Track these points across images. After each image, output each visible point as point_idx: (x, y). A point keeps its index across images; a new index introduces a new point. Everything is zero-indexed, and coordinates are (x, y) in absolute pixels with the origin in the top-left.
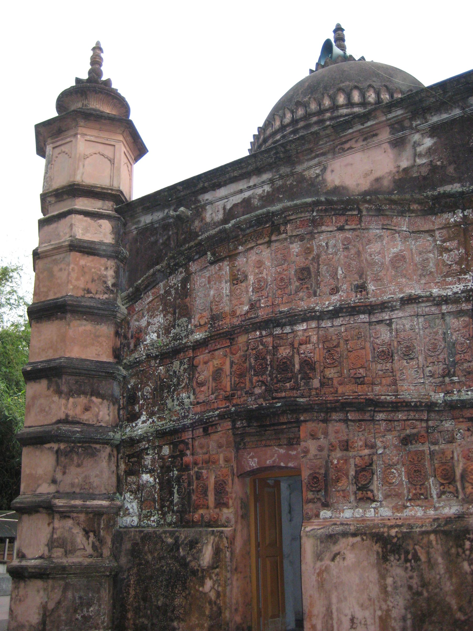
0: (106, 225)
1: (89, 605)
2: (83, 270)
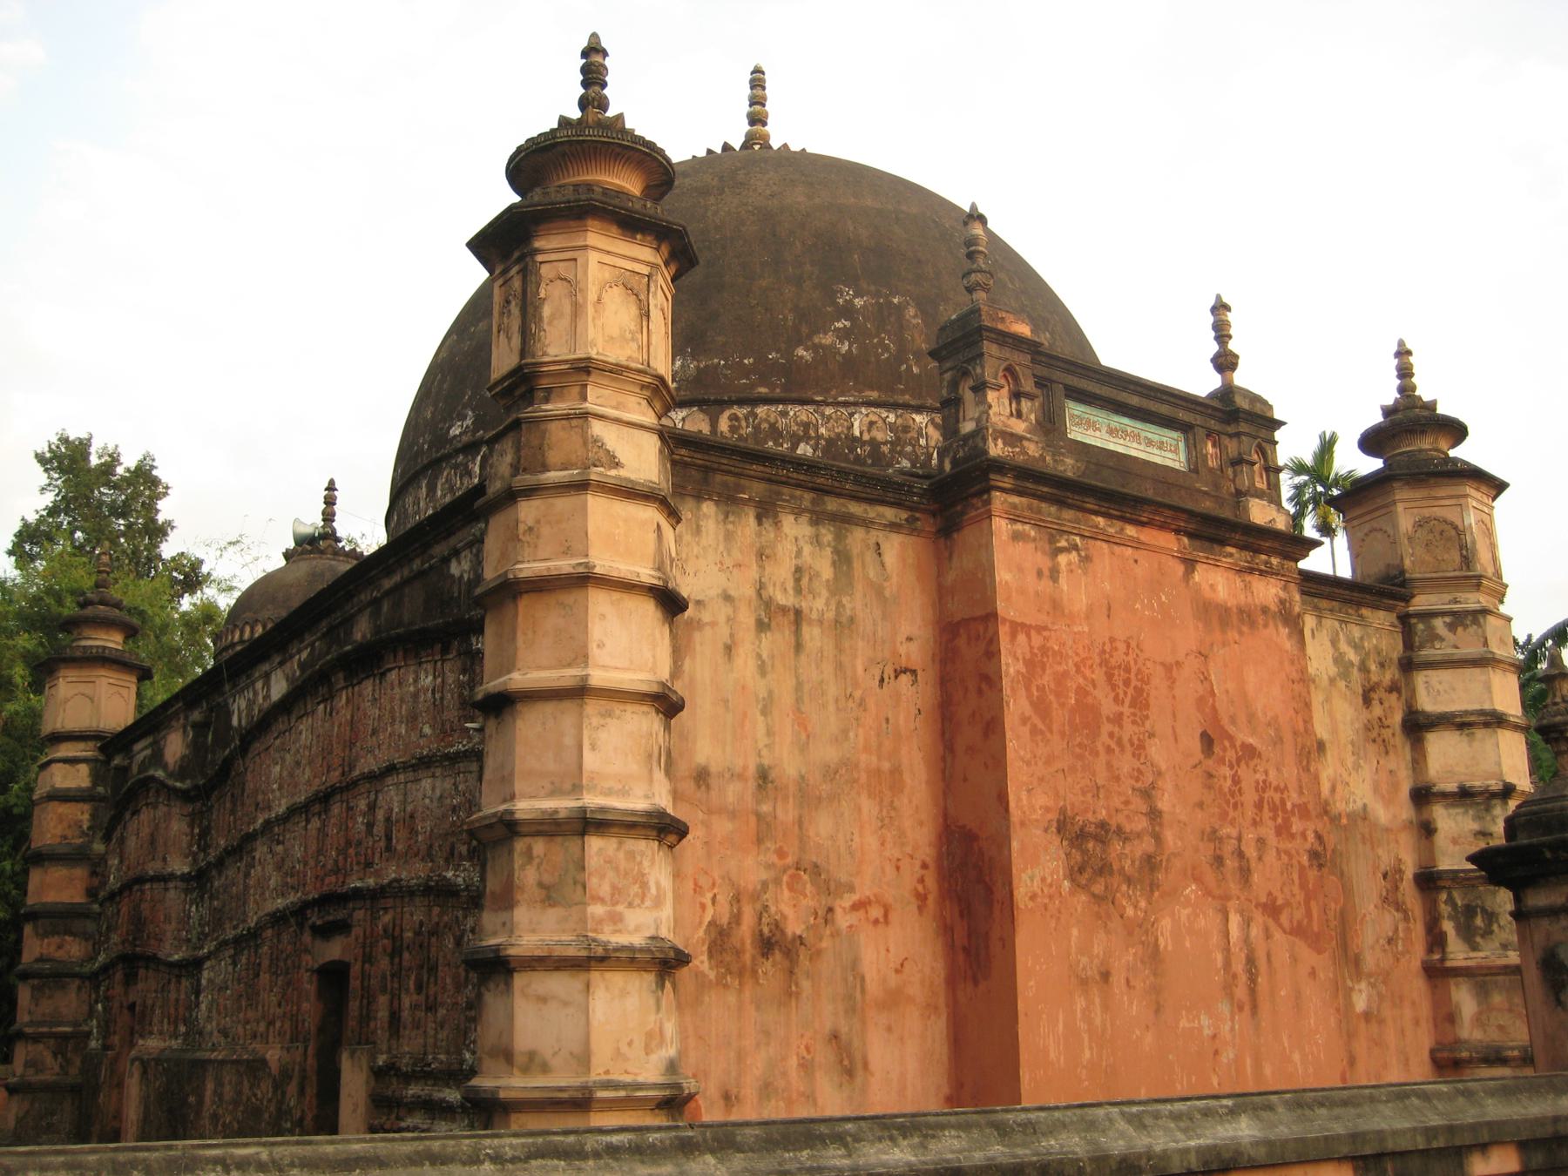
0: (84, 769)
1: (52, 1114)
2: (61, 819)
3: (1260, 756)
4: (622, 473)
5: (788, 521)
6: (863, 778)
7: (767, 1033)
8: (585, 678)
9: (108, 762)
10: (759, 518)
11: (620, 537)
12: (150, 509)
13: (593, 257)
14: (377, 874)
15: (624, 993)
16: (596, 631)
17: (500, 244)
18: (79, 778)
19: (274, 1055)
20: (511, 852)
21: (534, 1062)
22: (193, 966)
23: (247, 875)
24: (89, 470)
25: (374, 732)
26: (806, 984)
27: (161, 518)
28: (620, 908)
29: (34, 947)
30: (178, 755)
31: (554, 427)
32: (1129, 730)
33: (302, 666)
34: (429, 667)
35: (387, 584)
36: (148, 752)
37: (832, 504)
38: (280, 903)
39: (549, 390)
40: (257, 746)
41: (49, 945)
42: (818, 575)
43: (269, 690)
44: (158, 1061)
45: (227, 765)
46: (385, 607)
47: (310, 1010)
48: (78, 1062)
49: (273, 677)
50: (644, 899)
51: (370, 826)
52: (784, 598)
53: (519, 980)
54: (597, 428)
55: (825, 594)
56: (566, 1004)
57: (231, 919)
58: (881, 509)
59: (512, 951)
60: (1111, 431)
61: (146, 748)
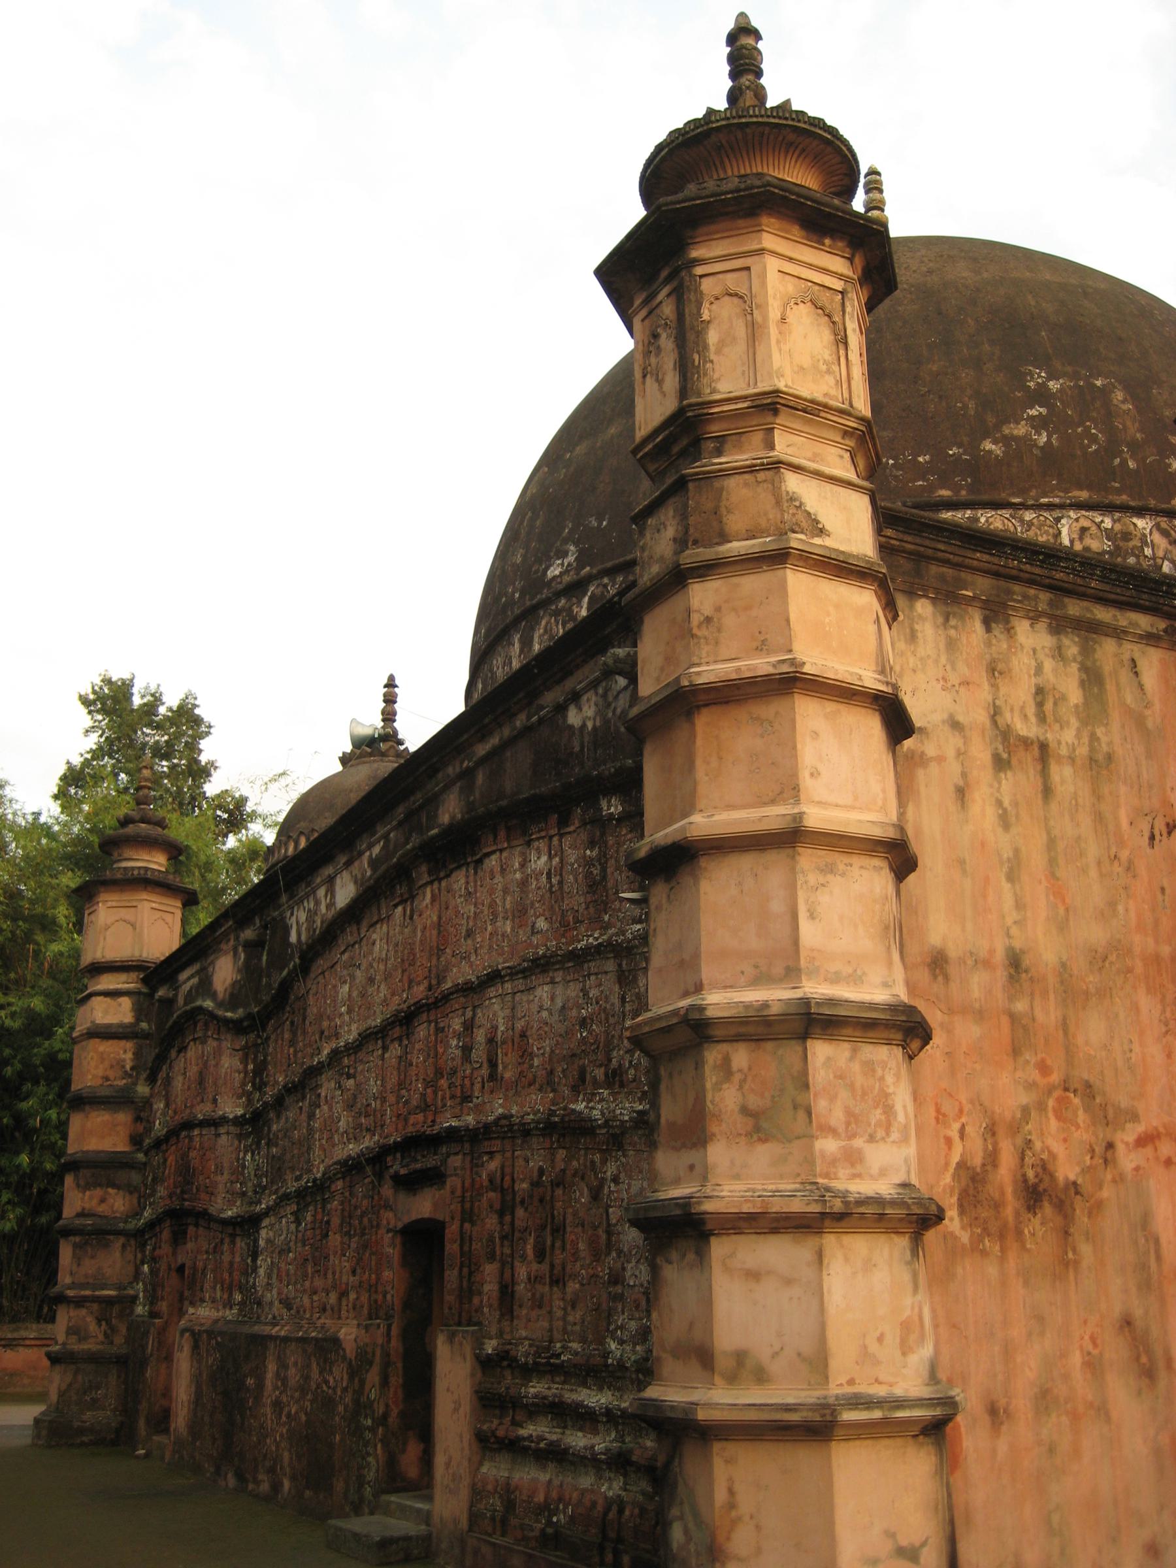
0: (126, 1003)
1: (98, 1388)
4: (828, 542)
5: (1022, 627)
6: (1139, 968)
7: (1040, 1319)
8: (801, 815)
9: (151, 995)
10: (987, 623)
11: (832, 626)
12: (193, 748)
13: (772, 265)
14: (478, 1109)
15: (869, 1266)
16: (808, 754)
17: (641, 272)
18: (120, 1012)
19: (349, 1333)
20: (699, 1065)
21: (745, 1367)
22: (249, 1224)
23: (311, 1116)
24: (133, 710)
25: (469, 934)
26: (1085, 1249)
27: (203, 759)
28: (858, 1143)
29: (76, 1200)
30: (229, 981)
31: (732, 483)
33: (374, 863)
34: (542, 845)
35: (482, 750)
36: (195, 980)
37: (1074, 608)
38: (353, 1149)
39: (721, 440)
40: (321, 963)
41: (91, 1198)
42: (1063, 698)
43: (333, 896)
44: (210, 1333)
45: (285, 988)
46: (480, 778)
47: (393, 1279)
48: (123, 1329)
49: (338, 881)
50: (880, 1131)
51: (467, 1050)
52: (1026, 728)
53: (719, 1248)
54: (793, 483)
55: (1074, 723)
56: (789, 1282)
57: (293, 1169)
58: (1134, 616)
59: (708, 1207)
61: (192, 976)
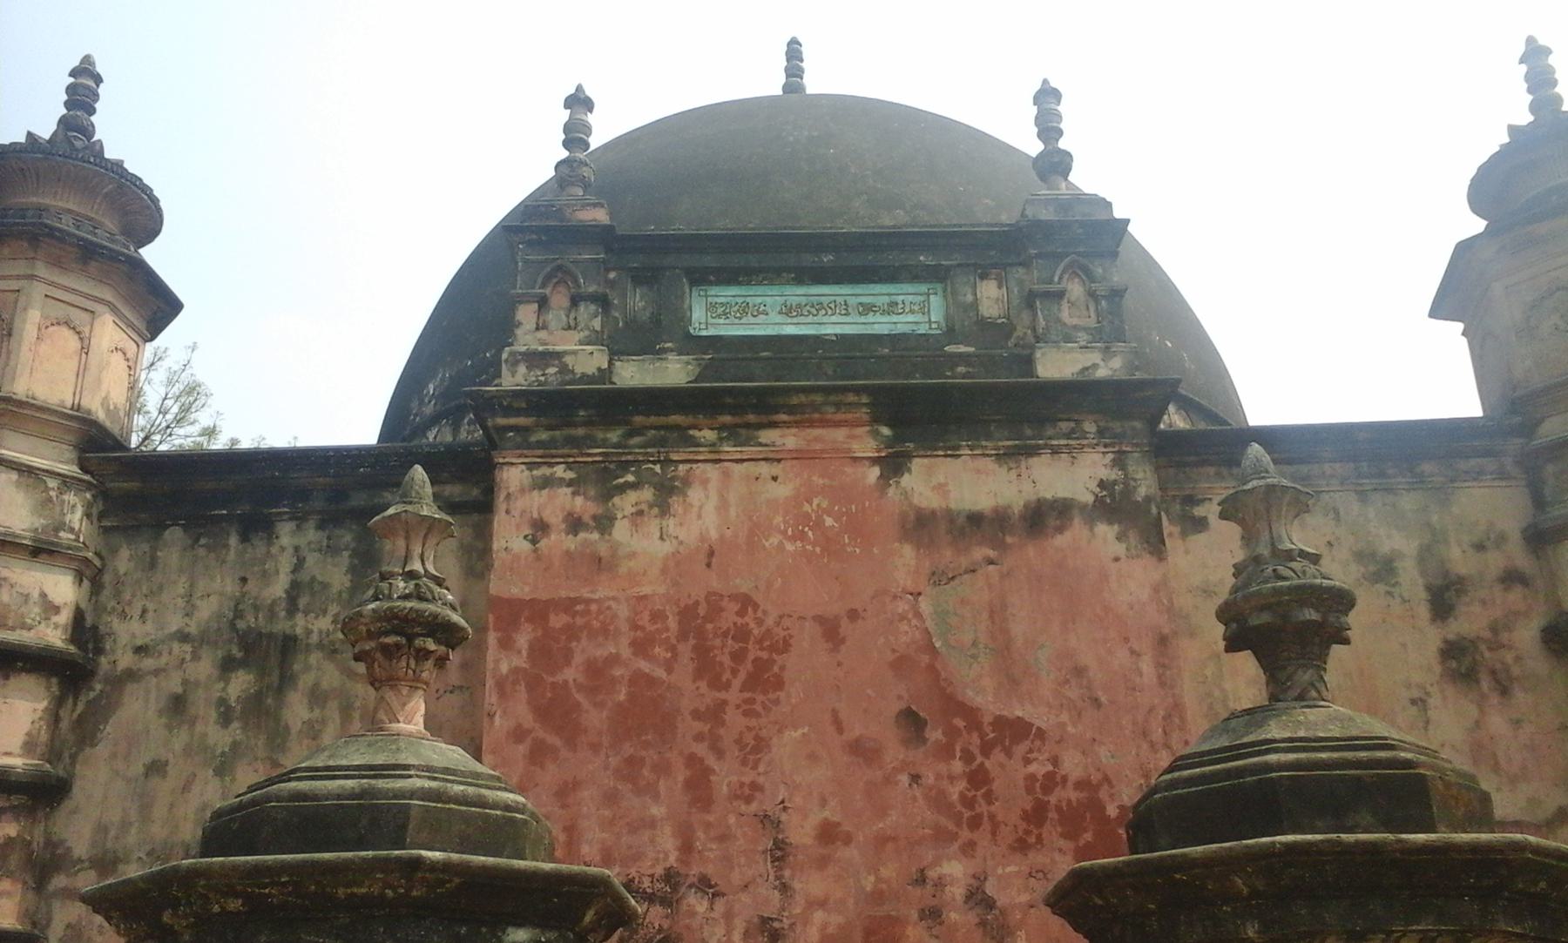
3: (1041, 734)
10: (245, 538)
32: (735, 720)
60: (787, 311)
